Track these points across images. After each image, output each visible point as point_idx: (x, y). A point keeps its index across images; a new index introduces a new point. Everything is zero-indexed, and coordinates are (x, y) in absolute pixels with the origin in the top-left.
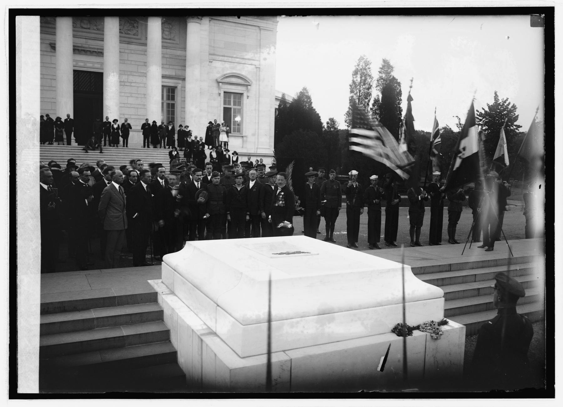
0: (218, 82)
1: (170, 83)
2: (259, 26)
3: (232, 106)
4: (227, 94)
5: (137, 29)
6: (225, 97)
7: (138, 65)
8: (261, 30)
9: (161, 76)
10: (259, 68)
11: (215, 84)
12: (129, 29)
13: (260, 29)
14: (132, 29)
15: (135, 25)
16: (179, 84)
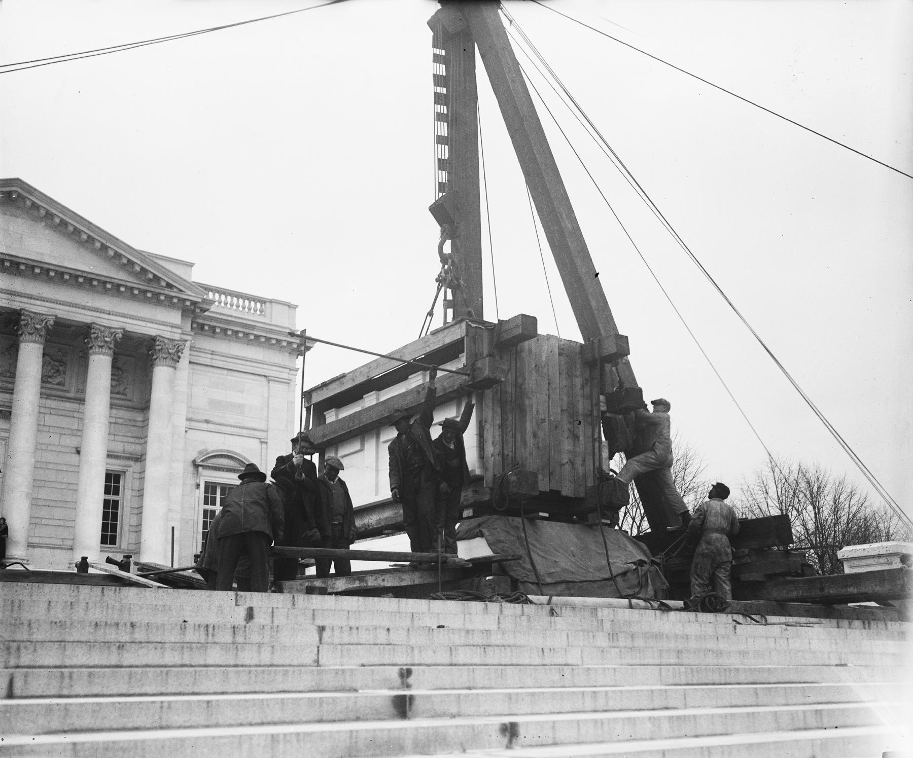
0: (195, 465)
1: (116, 465)
2: (265, 376)
4: (210, 488)
5: (63, 376)
6: (206, 491)
7: (61, 434)
8: (271, 382)
9: (106, 453)
10: (267, 443)
11: (191, 469)
12: (50, 374)
13: (269, 381)
14: (55, 375)
15: (61, 368)
16: (130, 466)
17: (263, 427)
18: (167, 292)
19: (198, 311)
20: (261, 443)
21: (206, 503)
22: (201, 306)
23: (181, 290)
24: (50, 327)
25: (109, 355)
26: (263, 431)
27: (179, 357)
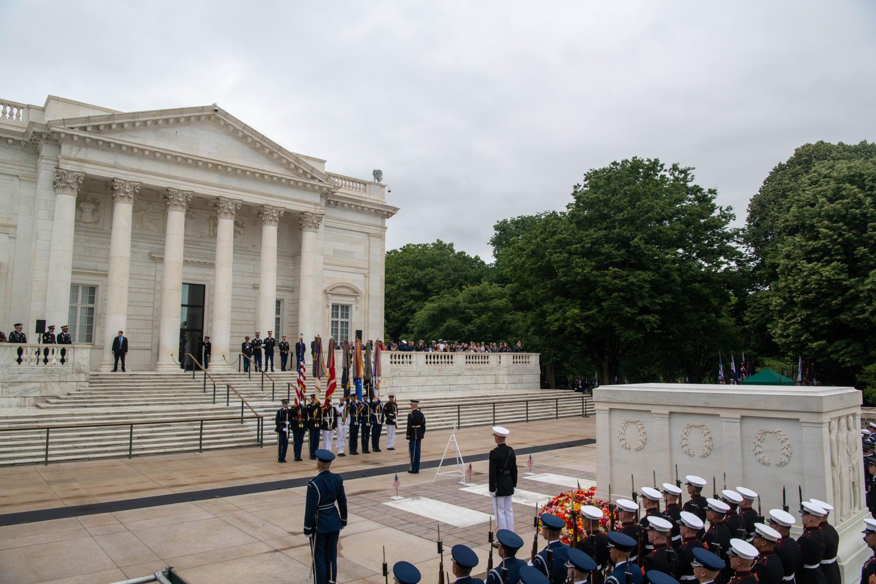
3: (340, 319)
4: (335, 307)
6: (333, 310)
9: (275, 288)
10: (369, 277)
15: (242, 232)
17: (367, 266)
18: (313, 182)
19: (330, 193)
20: (365, 277)
21: (333, 317)
22: (333, 190)
23: (320, 181)
24: (239, 208)
25: (275, 226)
26: (366, 269)
27: (319, 225)
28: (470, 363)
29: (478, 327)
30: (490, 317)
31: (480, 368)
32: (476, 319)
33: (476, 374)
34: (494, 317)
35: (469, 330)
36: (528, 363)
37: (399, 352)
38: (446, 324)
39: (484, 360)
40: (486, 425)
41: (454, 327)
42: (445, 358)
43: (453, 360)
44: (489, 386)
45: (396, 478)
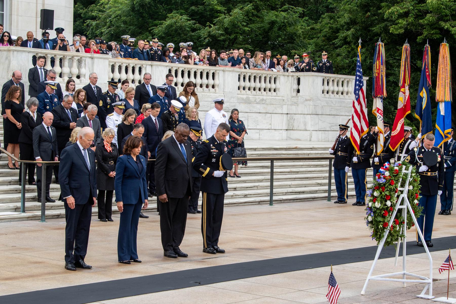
28: (244, 89)
29: (226, 29)
30: (247, 14)
31: (263, 100)
32: (223, 16)
33: (255, 110)
34: (255, 13)
35: (210, 36)
36: (347, 93)
37: (125, 62)
38: (168, 22)
39: (268, 86)
40: (314, 199)
41: (181, 28)
42: (201, 77)
43: (217, 81)
44: (277, 135)
45: (332, 281)
